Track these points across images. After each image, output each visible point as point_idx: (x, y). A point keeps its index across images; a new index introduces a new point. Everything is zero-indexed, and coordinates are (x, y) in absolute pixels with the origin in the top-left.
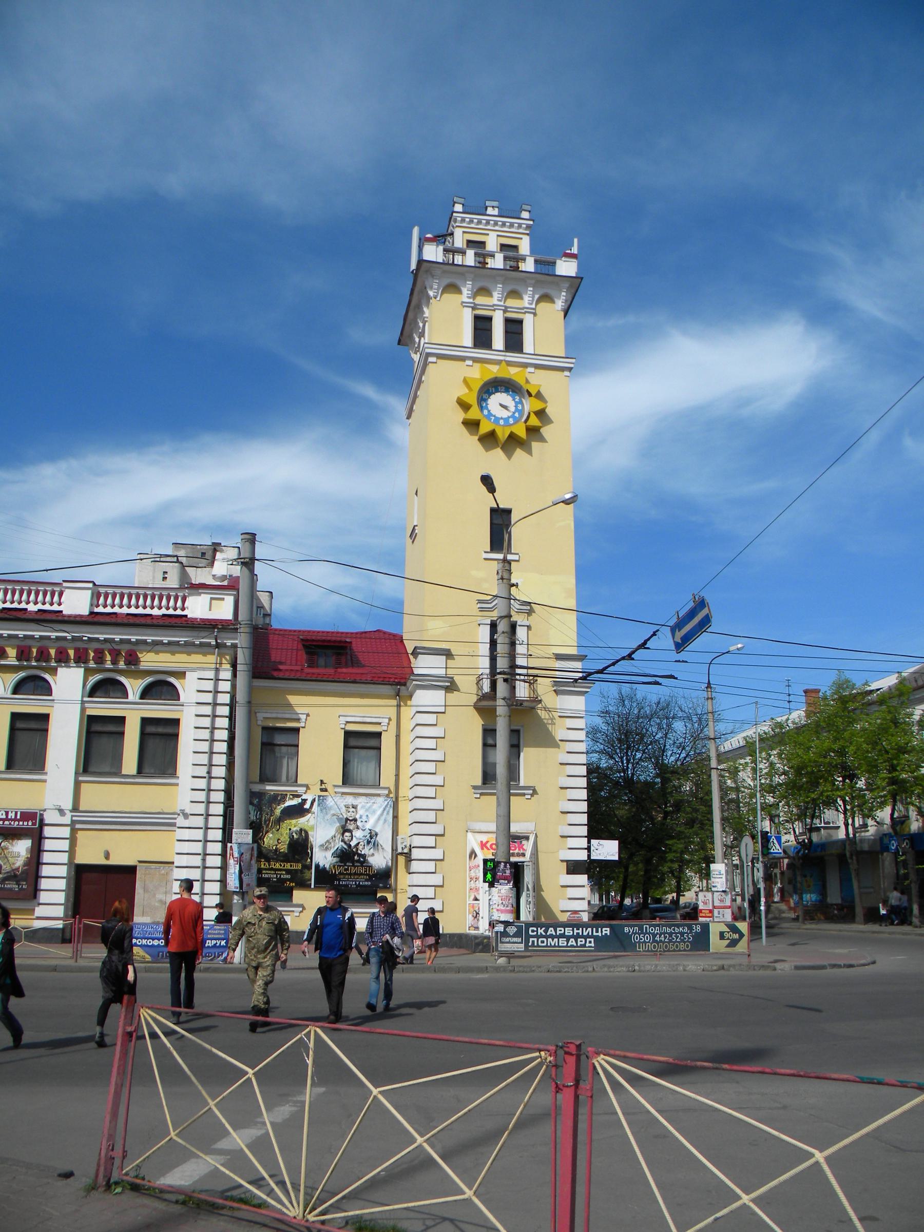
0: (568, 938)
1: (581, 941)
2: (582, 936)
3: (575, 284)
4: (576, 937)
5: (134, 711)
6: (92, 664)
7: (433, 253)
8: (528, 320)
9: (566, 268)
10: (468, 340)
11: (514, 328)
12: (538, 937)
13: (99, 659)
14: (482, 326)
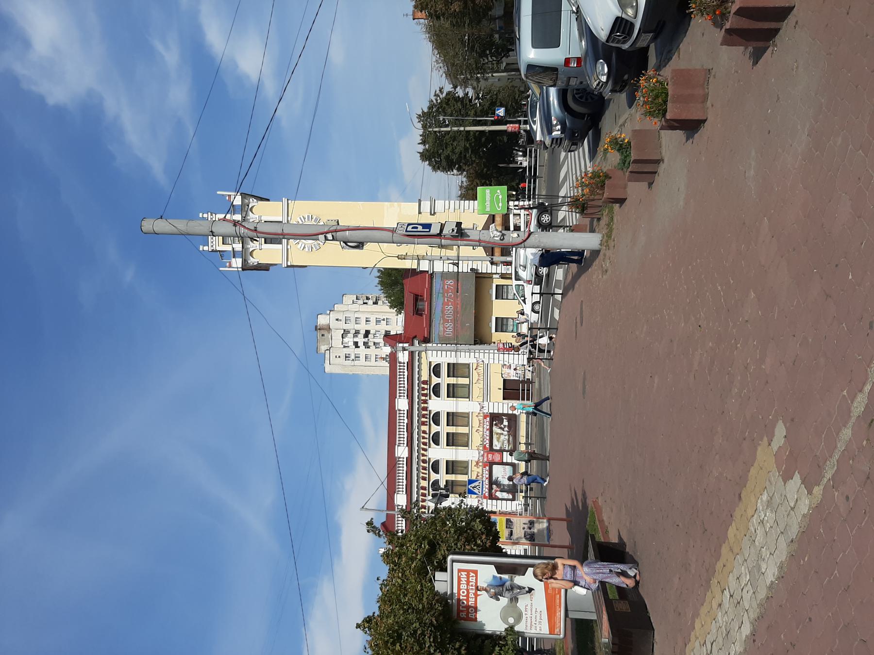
3: (244, 196)
5: (445, 380)
6: (428, 398)
7: (237, 263)
9: (238, 201)
10: (279, 246)
13: (425, 395)
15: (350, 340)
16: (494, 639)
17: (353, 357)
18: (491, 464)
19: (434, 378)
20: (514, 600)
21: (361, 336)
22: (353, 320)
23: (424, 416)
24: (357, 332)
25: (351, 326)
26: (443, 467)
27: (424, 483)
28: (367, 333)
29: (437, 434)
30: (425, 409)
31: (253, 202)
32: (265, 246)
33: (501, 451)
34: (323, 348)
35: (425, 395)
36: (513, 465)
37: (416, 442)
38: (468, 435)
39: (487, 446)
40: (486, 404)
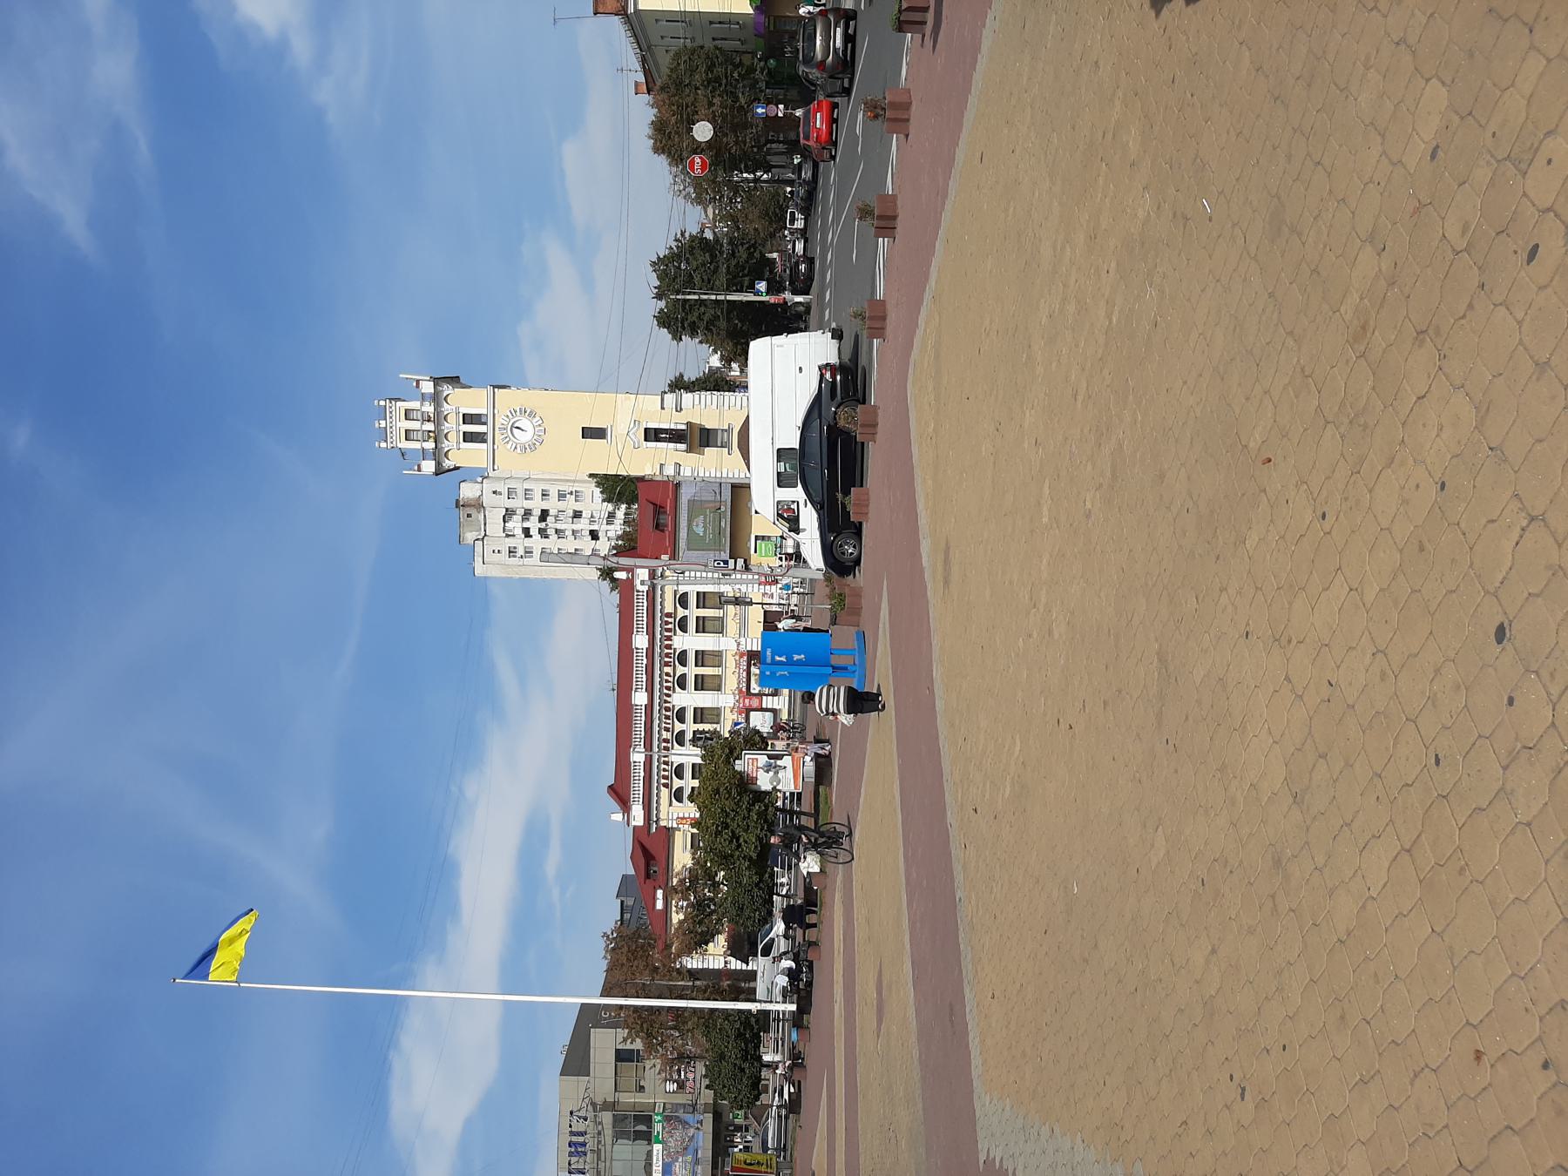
3: (437, 381)
5: (693, 612)
7: (429, 466)
8: (464, 410)
9: (428, 387)
10: (484, 446)
11: (468, 419)
13: (669, 630)
14: (469, 437)
15: (516, 525)
16: (767, 793)
17: (521, 552)
18: (748, 711)
19: (680, 609)
20: (776, 773)
21: (534, 519)
22: (521, 493)
23: (667, 655)
24: (527, 514)
25: (519, 504)
26: (689, 715)
27: (665, 735)
28: (544, 515)
29: (683, 676)
30: (669, 647)
31: (447, 389)
32: (464, 445)
33: (760, 695)
34: (470, 537)
35: (669, 630)
36: (774, 711)
37: (657, 686)
38: (719, 677)
40: (742, 640)
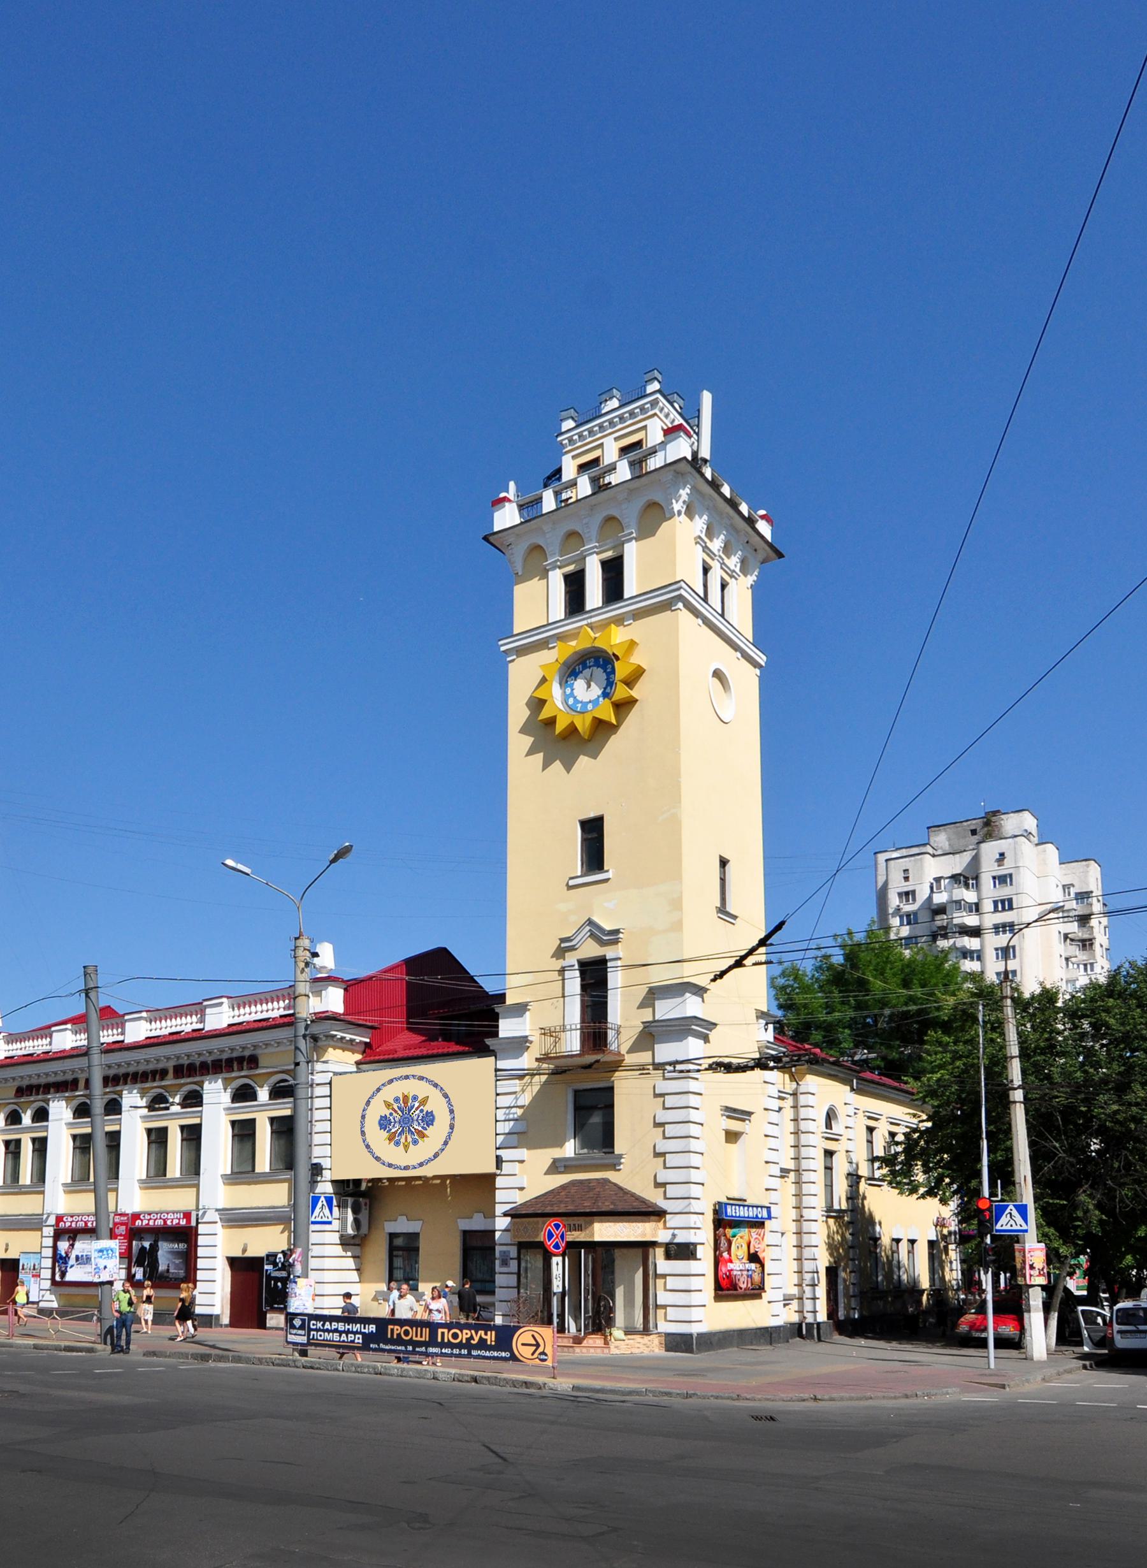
0: (341, 1333)
1: (351, 1337)
2: (352, 1332)
4: (347, 1332)
12: (317, 1330)
39: (138, 1223)
